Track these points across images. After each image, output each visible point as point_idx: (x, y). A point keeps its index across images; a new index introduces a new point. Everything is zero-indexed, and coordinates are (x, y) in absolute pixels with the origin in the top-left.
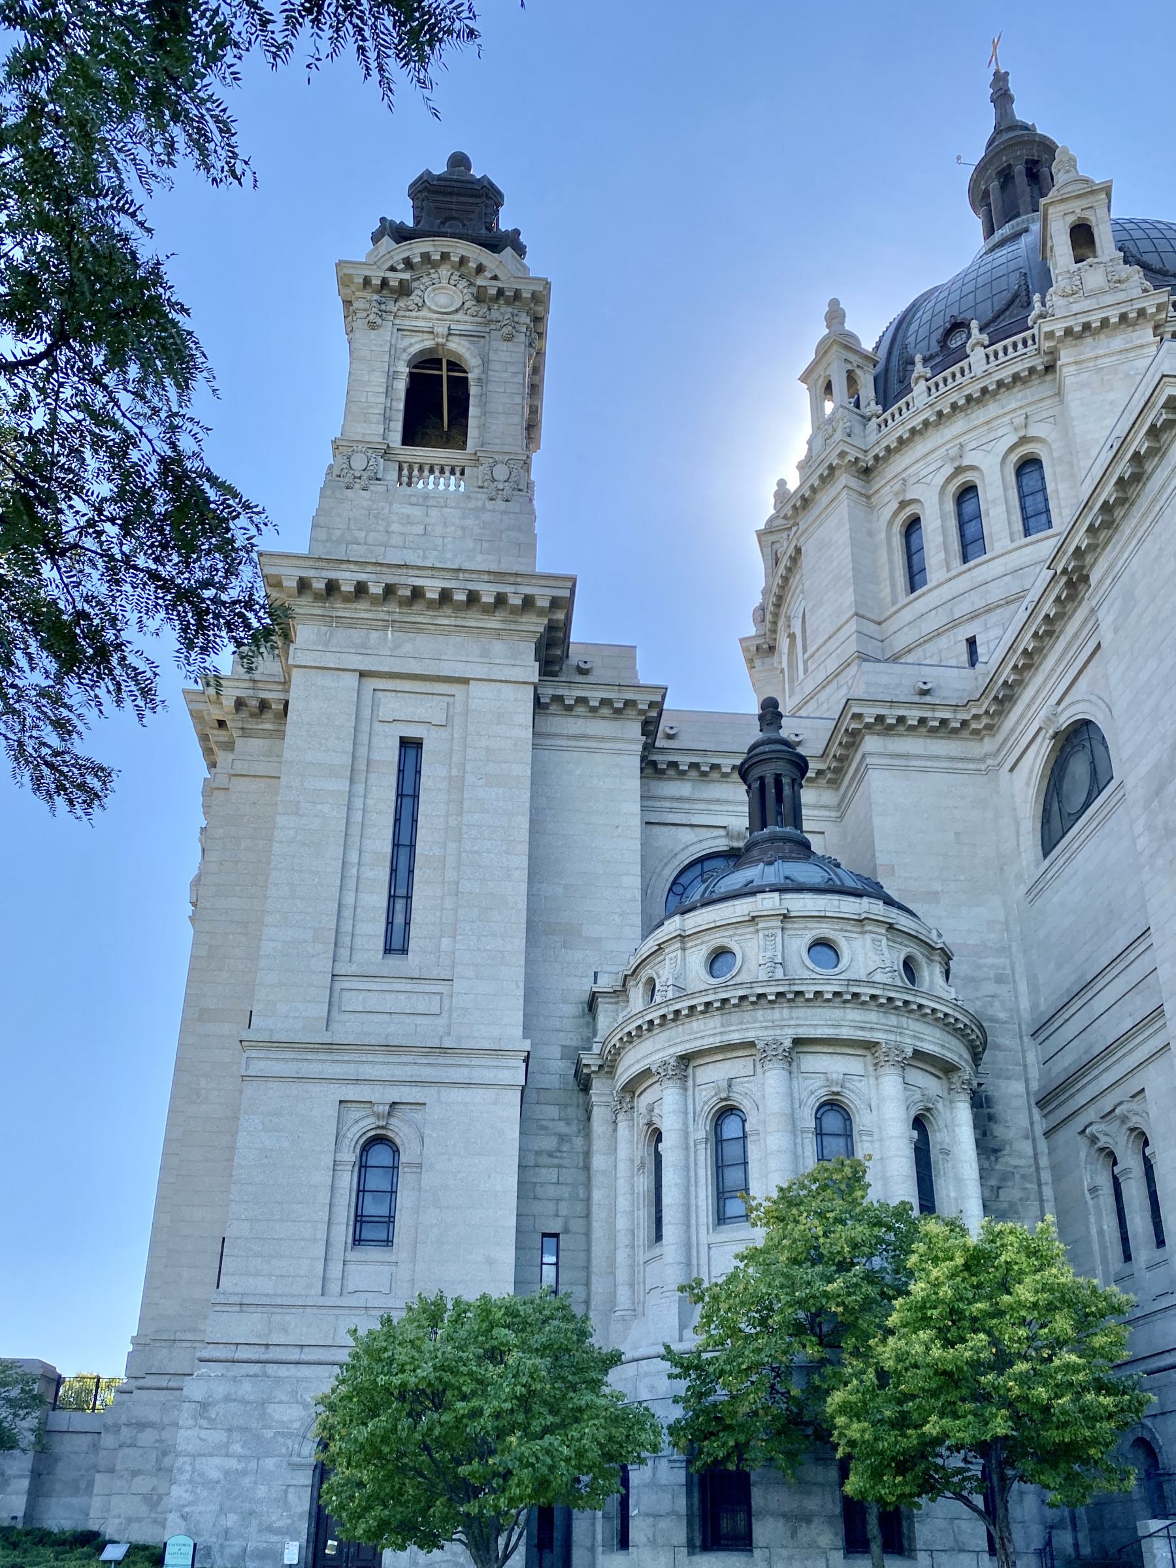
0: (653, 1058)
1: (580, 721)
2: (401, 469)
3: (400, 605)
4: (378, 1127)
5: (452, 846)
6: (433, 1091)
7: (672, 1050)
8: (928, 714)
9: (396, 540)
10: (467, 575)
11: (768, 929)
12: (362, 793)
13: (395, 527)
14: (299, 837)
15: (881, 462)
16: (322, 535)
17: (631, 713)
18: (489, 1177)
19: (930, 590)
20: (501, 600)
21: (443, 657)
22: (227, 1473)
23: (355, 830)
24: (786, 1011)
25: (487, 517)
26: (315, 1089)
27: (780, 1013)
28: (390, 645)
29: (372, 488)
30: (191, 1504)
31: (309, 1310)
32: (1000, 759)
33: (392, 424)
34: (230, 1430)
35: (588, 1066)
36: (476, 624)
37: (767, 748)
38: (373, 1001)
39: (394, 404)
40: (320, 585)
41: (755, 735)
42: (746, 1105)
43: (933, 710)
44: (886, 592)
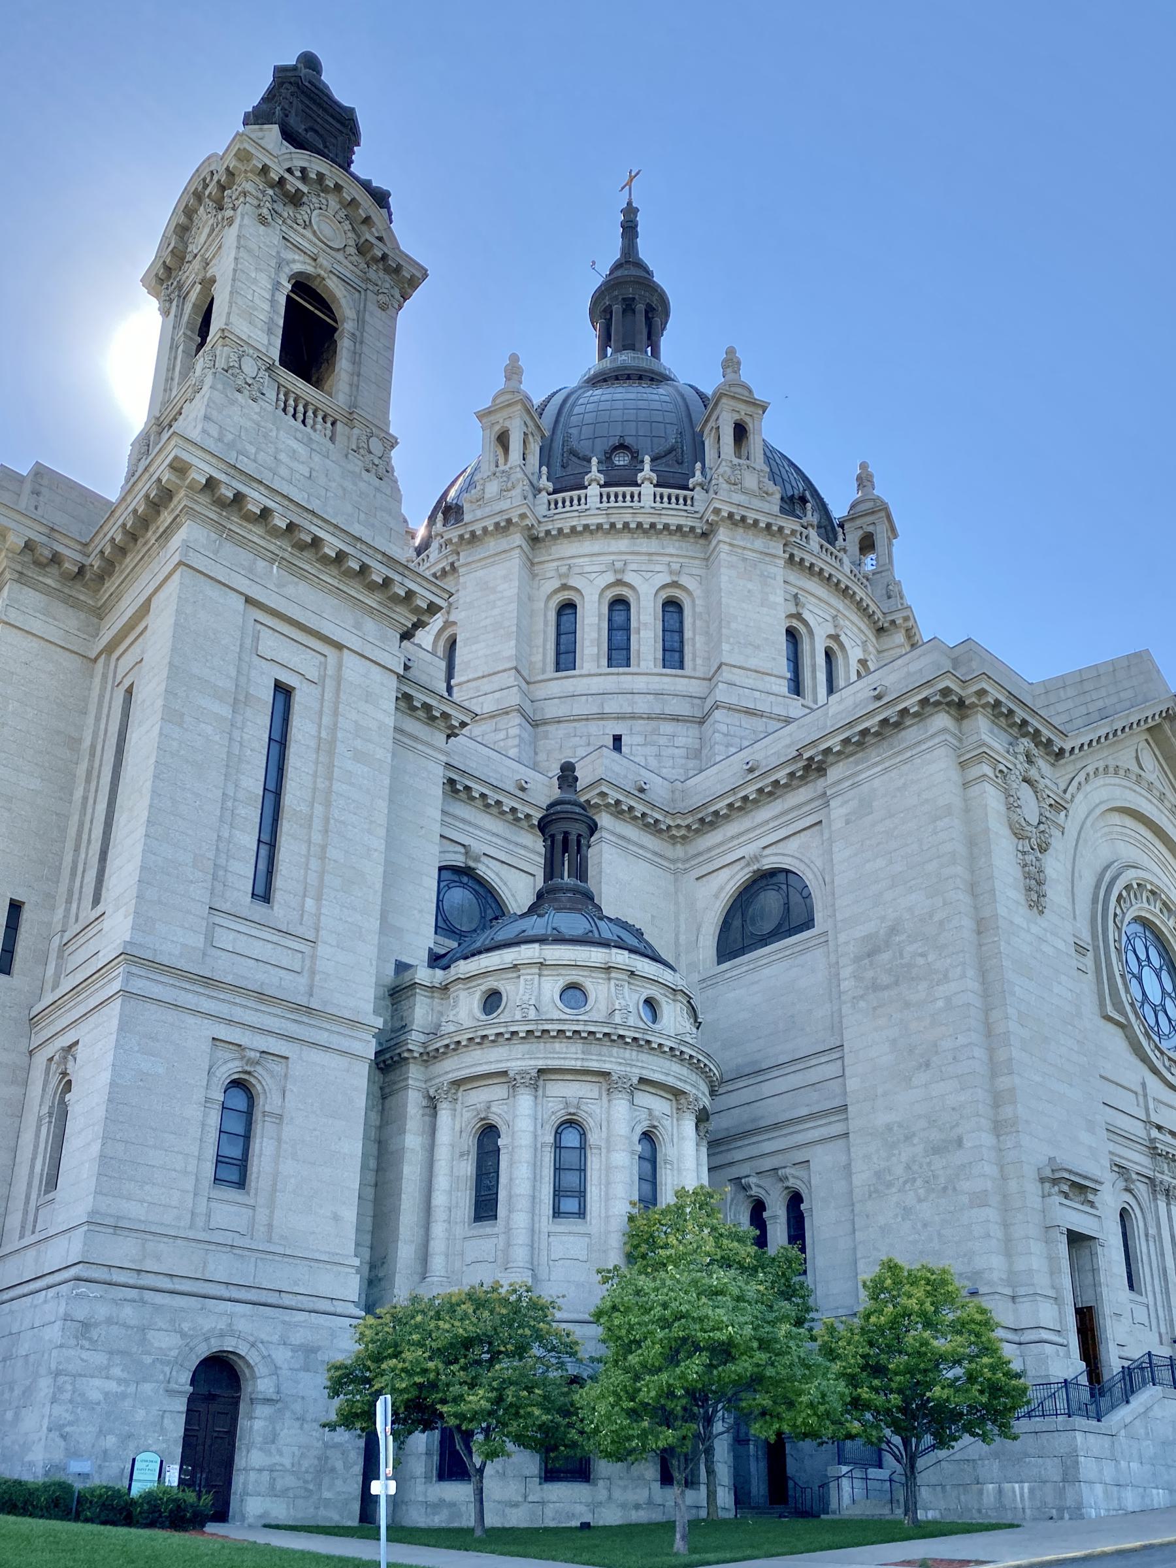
0: (514, 1064)
5: (319, 809)
6: (296, 1047)
7: (532, 1063)
8: (648, 812)
11: (617, 979)
14: (182, 752)
15: (549, 538)
19: (581, 676)
22: (106, 1394)
24: (634, 1053)
26: (191, 1020)
27: (629, 1054)
30: (70, 1424)
31: (179, 1241)
32: (687, 866)
34: (111, 1353)
35: (410, 1051)
38: (242, 944)
41: (556, 793)
42: (590, 1124)
44: (538, 658)
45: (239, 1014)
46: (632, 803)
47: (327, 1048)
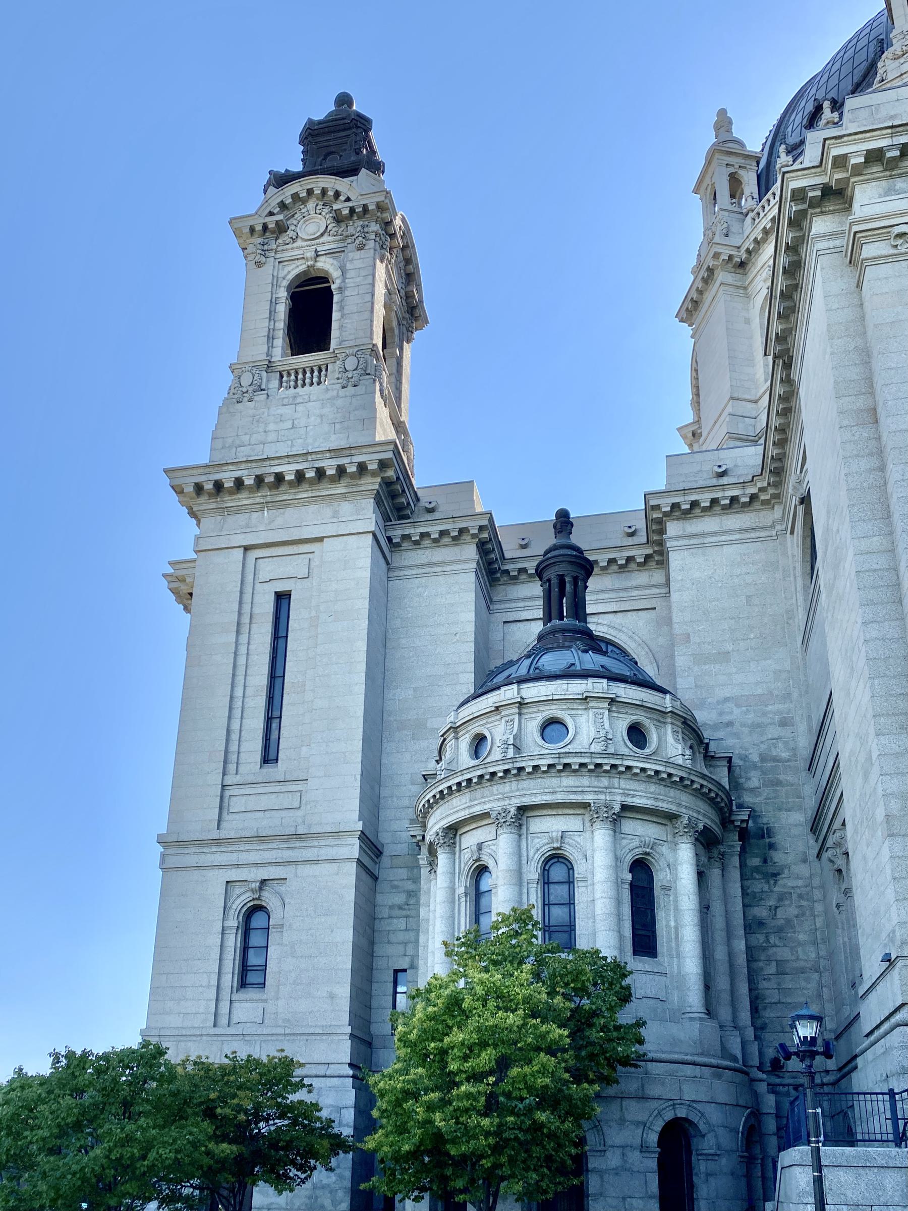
1: (428, 552)
2: (282, 377)
3: (270, 489)
4: (254, 899)
9: (272, 437)
10: (314, 456)
12: (246, 641)
13: (271, 427)
16: (219, 444)
17: (466, 538)
18: (332, 931)
20: (341, 471)
21: (304, 524)
23: (241, 671)
25: (339, 402)
26: (211, 873)
28: (266, 521)
29: (256, 398)
33: (275, 341)
36: (327, 493)
37: (562, 552)
39: (277, 324)
40: (209, 486)
43: (723, 490)
45: (245, 858)
46: (694, 498)
47: (317, 861)
